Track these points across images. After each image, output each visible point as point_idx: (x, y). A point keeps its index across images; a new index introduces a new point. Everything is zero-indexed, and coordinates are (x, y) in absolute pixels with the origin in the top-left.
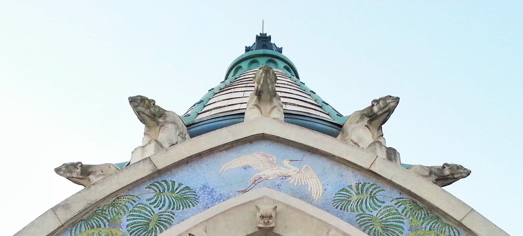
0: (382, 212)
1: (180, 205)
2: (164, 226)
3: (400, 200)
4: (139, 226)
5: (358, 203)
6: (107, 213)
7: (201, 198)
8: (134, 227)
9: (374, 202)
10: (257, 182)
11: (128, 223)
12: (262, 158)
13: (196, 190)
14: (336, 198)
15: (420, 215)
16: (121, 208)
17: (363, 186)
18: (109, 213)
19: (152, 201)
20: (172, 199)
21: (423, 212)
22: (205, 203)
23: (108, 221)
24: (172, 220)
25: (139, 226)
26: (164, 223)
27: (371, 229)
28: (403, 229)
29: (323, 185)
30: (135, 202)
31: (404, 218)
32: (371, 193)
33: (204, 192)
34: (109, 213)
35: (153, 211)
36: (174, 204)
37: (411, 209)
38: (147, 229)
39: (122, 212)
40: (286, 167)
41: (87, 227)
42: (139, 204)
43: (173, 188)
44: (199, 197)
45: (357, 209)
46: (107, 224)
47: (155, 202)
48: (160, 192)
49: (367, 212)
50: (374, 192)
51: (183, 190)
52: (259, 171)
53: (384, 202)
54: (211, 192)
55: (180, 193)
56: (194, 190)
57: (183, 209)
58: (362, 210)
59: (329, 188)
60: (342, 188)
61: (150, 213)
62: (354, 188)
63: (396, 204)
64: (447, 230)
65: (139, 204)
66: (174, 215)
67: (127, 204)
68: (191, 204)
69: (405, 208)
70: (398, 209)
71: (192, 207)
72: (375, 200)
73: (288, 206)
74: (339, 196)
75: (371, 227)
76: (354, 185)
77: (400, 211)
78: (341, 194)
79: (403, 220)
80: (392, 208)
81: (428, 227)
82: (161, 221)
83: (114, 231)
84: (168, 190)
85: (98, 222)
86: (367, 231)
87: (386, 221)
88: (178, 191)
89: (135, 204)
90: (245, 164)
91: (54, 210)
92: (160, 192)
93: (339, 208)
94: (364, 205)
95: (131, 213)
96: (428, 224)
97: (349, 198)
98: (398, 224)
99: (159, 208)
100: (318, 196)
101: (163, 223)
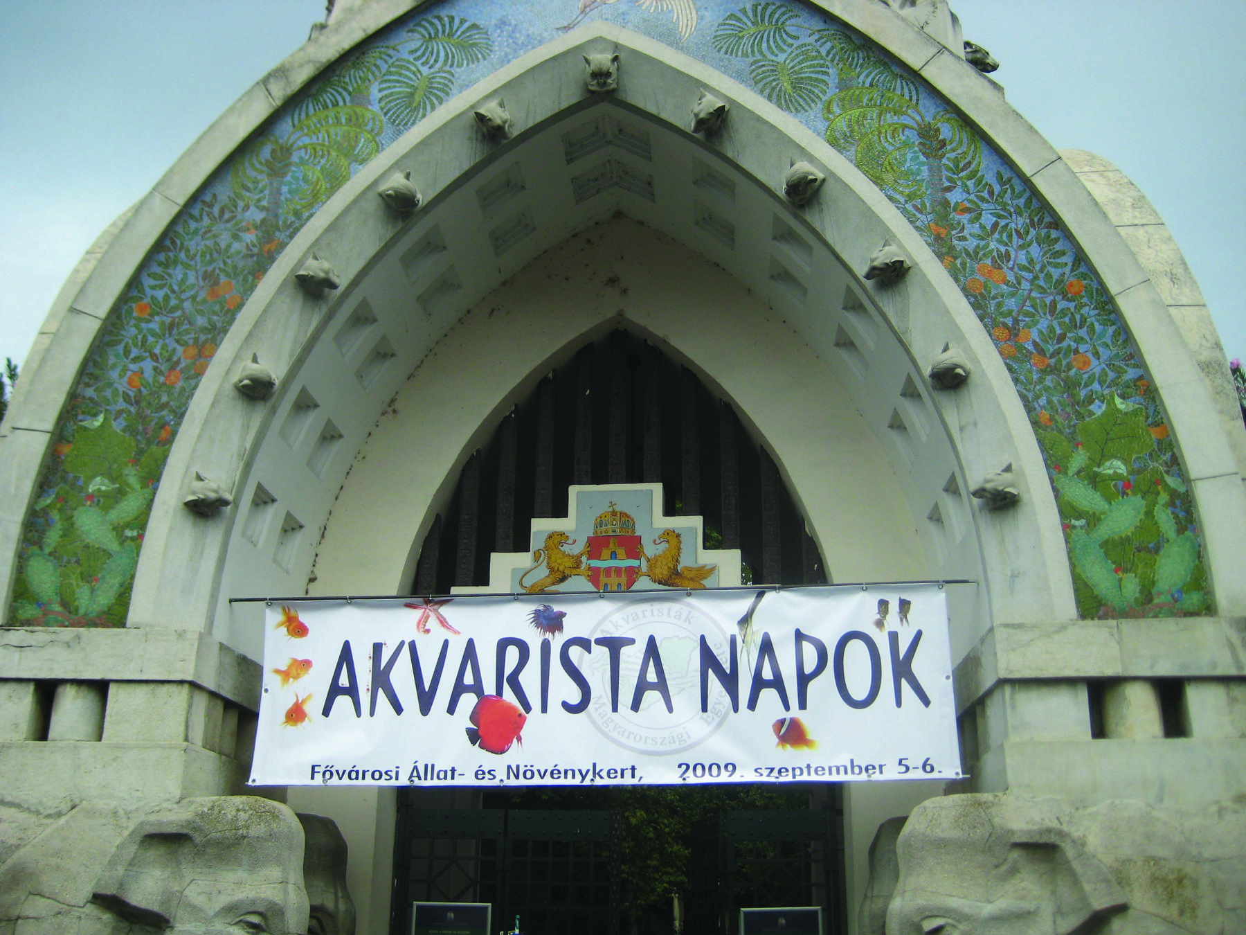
0: (793, 55)
1: (462, 59)
2: (437, 97)
3: (825, 33)
4: (398, 99)
5: (754, 40)
6: (347, 80)
7: (496, 44)
8: (390, 102)
9: (781, 37)
10: (588, 10)
11: (380, 95)
13: (488, 30)
14: (719, 33)
15: (856, 59)
16: (368, 69)
17: (765, 9)
18: (350, 80)
19: (419, 53)
20: (451, 49)
21: (861, 55)
22: (503, 53)
23: (350, 94)
24: (451, 86)
25: (398, 99)
26: (439, 93)
27: (774, 89)
30: (391, 57)
31: (830, 65)
32: (777, 21)
33: (502, 32)
34: (350, 80)
35: (419, 71)
36: (453, 57)
37: (842, 49)
38: (411, 104)
39: (371, 77)
41: (317, 108)
42: (397, 60)
43: (451, 27)
44: (493, 42)
45: (753, 52)
46: (348, 98)
47: (423, 54)
48: (430, 36)
50: (782, 20)
51: (469, 29)
54: (513, 32)
55: (462, 37)
56: (485, 31)
57: (468, 64)
58: (761, 52)
60: (729, 14)
61: (416, 76)
62: (750, 14)
63: (817, 41)
64: (898, 86)
65: (397, 60)
66: (453, 76)
67: (379, 62)
68: (480, 56)
69: (833, 48)
70: (820, 49)
71: (481, 60)
72: (784, 35)
74: (723, 30)
75: (774, 83)
76: (748, 7)
77: (824, 53)
78: (728, 24)
79: (827, 70)
80: (810, 48)
81: (868, 81)
82: (433, 88)
83: (359, 110)
84: (444, 32)
85: (334, 97)
86: (767, 91)
88: (459, 33)
89: (390, 61)
91: (265, 81)
92: (430, 34)
93: (723, 50)
94: (764, 45)
95: (386, 78)
96: (867, 76)
97: (740, 32)
98: (820, 76)
99: (429, 66)
100: (689, 30)
101: (436, 91)
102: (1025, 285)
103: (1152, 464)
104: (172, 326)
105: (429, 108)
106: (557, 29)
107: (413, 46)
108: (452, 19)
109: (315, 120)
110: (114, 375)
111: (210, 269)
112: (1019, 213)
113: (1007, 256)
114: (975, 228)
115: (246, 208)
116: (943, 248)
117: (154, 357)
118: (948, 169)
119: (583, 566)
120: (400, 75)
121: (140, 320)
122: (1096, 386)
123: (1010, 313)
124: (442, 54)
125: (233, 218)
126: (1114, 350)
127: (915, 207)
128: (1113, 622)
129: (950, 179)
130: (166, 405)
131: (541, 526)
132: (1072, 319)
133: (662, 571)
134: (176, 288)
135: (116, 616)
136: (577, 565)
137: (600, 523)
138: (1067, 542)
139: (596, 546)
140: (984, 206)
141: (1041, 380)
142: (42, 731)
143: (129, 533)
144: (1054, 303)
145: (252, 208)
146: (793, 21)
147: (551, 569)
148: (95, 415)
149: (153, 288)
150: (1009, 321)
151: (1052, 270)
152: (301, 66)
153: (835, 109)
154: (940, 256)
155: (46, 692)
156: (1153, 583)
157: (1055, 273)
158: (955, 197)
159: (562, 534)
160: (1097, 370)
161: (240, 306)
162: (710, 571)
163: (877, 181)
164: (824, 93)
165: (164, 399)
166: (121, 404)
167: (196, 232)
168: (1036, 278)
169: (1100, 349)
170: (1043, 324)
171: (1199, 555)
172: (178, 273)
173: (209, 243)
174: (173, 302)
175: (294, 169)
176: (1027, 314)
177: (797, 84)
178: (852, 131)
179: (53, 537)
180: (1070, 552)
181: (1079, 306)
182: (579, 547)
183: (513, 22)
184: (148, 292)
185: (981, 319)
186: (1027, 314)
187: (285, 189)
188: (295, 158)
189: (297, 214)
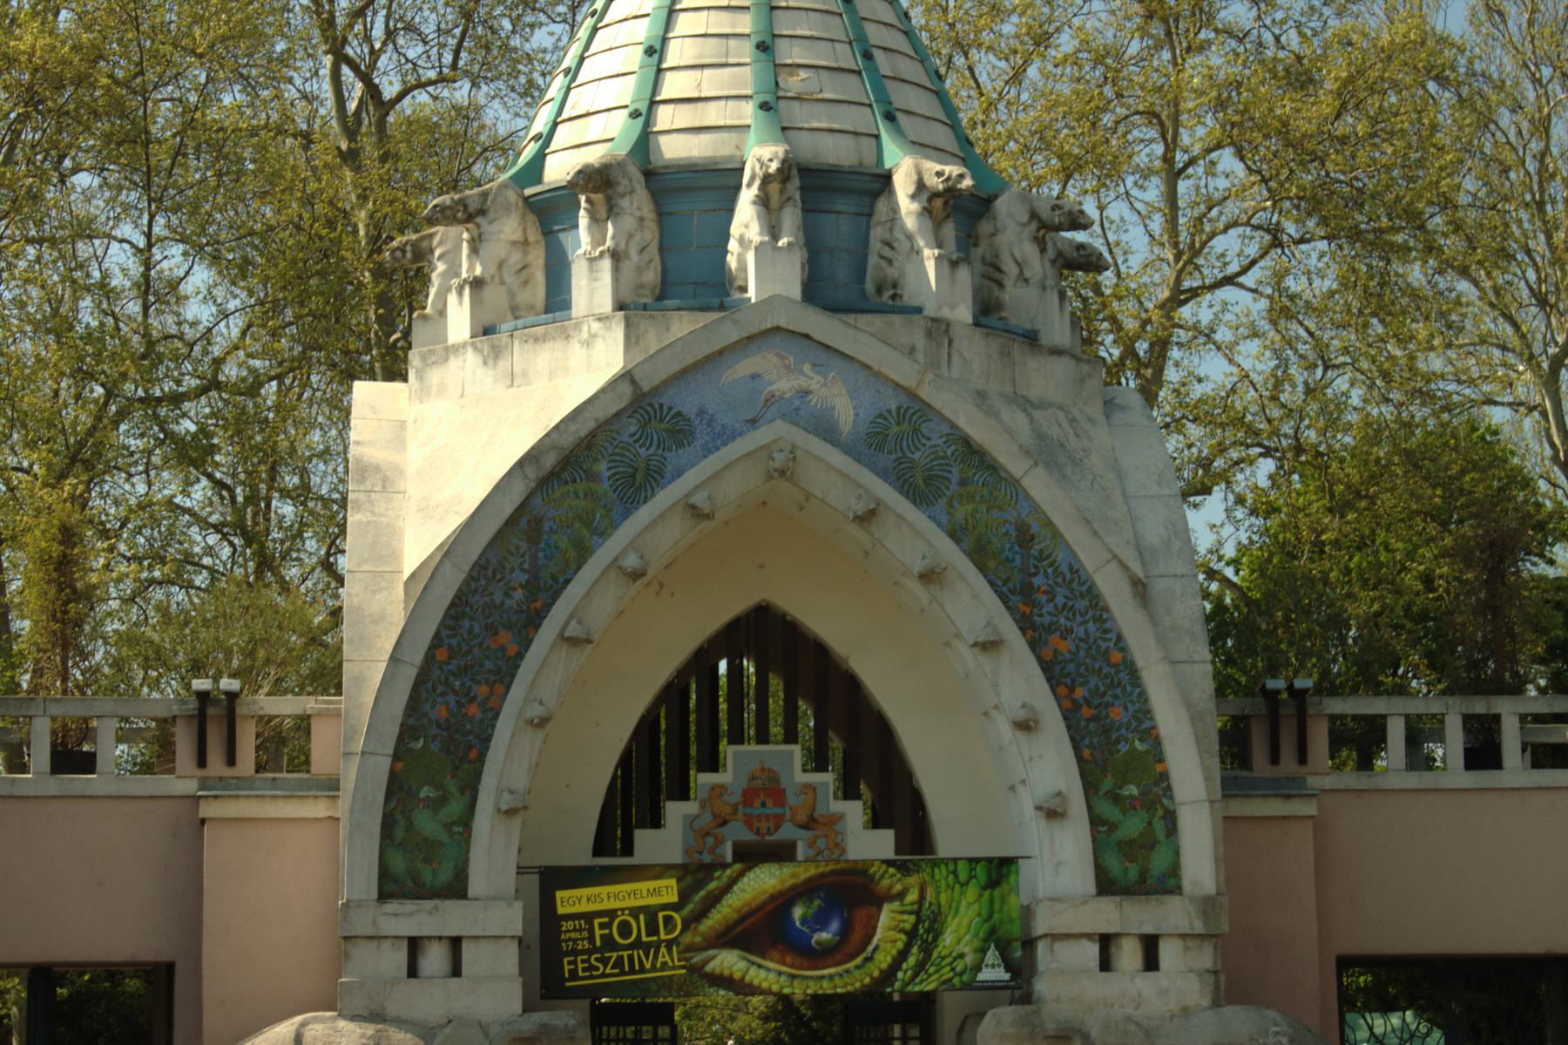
2: (655, 480)
11: (608, 474)
12: (775, 360)
28: (950, 482)
29: (855, 408)
40: (807, 376)
47: (640, 438)
49: (908, 454)
51: (673, 417)
52: (771, 383)
53: (929, 439)
59: (861, 411)
62: (894, 414)
73: (807, 452)
76: (893, 407)
77: (949, 454)
86: (906, 487)
87: (931, 469)
90: (752, 370)
94: (905, 443)
102: (1082, 653)
103: (1155, 789)
104: (466, 667)
105: (649, 493)
106: (747, 421)
107: (633, 429)
108: (661, 406)
109: (558, 493)
110: (427, 707)
111: (490, 620)
112: (1083, 597)
113: (1071, 631)
114: (1050, 608)
115: (512, 570)
116: (1025, 624)
117: (454, 691)
118: (1035, 558)
119: (740, 813)
120: (623, 456)
121: (440, 662)
122: (1123, 731)
123: (1069, 675)
124: (655, 437)
125: (503, 578)
126: (1138, 706)
127: (1009, 590)
128: (1118, 898)
129: (1036, 567)
130: (470, 732)
131: (702, 780)
132: (1112, 680)
133: (802, 817)
134: (465, 636)
135: (457, 889)
136: (735, 812)
137: (753, 778)
138: (1093, 842)
139: (749, 796)
140: (1058, 589)
141: (1086, 726)
142: (413, 972)
143: (456, 829)
144: (1100, 669)
145: (517, 571)
146: (927, 424)
147: (715, 816)
148: (417, 739)
149: (448, 637)
150: (1069, 681)
151: (1101, 643)
152: (548, 451)
153: (956, 503)
154: (1023, 630)
155: (415, 945)
156: (1148, 870)
157: (1104, 645)
158: (1038, 581)
159: (722, 787)
160: (1125, 720)
161: (520, 656)
162: (840, 818)
163: (982, 568)
164: (948, 488)
165: (468, 727)
166: (435, 731)
167: (476, 591)
168: (1090, 648)
169: (1129, 705)
170: (1094, 681)
172: (466, 623)
173: (487, 599)
174: (465, 648)
175: (545, 536)
176: (1081, 676)
177: (928, 480)
178: (967, 523)
179: (399, 832)
180: (1095, 849)
181: (1118, 672)
182: (736, 797)
183: (711, 412)
184: (447, 641)
185: (1048, 680)
186: (1081, 676)
187: (541, 555)
188: (546, 527)
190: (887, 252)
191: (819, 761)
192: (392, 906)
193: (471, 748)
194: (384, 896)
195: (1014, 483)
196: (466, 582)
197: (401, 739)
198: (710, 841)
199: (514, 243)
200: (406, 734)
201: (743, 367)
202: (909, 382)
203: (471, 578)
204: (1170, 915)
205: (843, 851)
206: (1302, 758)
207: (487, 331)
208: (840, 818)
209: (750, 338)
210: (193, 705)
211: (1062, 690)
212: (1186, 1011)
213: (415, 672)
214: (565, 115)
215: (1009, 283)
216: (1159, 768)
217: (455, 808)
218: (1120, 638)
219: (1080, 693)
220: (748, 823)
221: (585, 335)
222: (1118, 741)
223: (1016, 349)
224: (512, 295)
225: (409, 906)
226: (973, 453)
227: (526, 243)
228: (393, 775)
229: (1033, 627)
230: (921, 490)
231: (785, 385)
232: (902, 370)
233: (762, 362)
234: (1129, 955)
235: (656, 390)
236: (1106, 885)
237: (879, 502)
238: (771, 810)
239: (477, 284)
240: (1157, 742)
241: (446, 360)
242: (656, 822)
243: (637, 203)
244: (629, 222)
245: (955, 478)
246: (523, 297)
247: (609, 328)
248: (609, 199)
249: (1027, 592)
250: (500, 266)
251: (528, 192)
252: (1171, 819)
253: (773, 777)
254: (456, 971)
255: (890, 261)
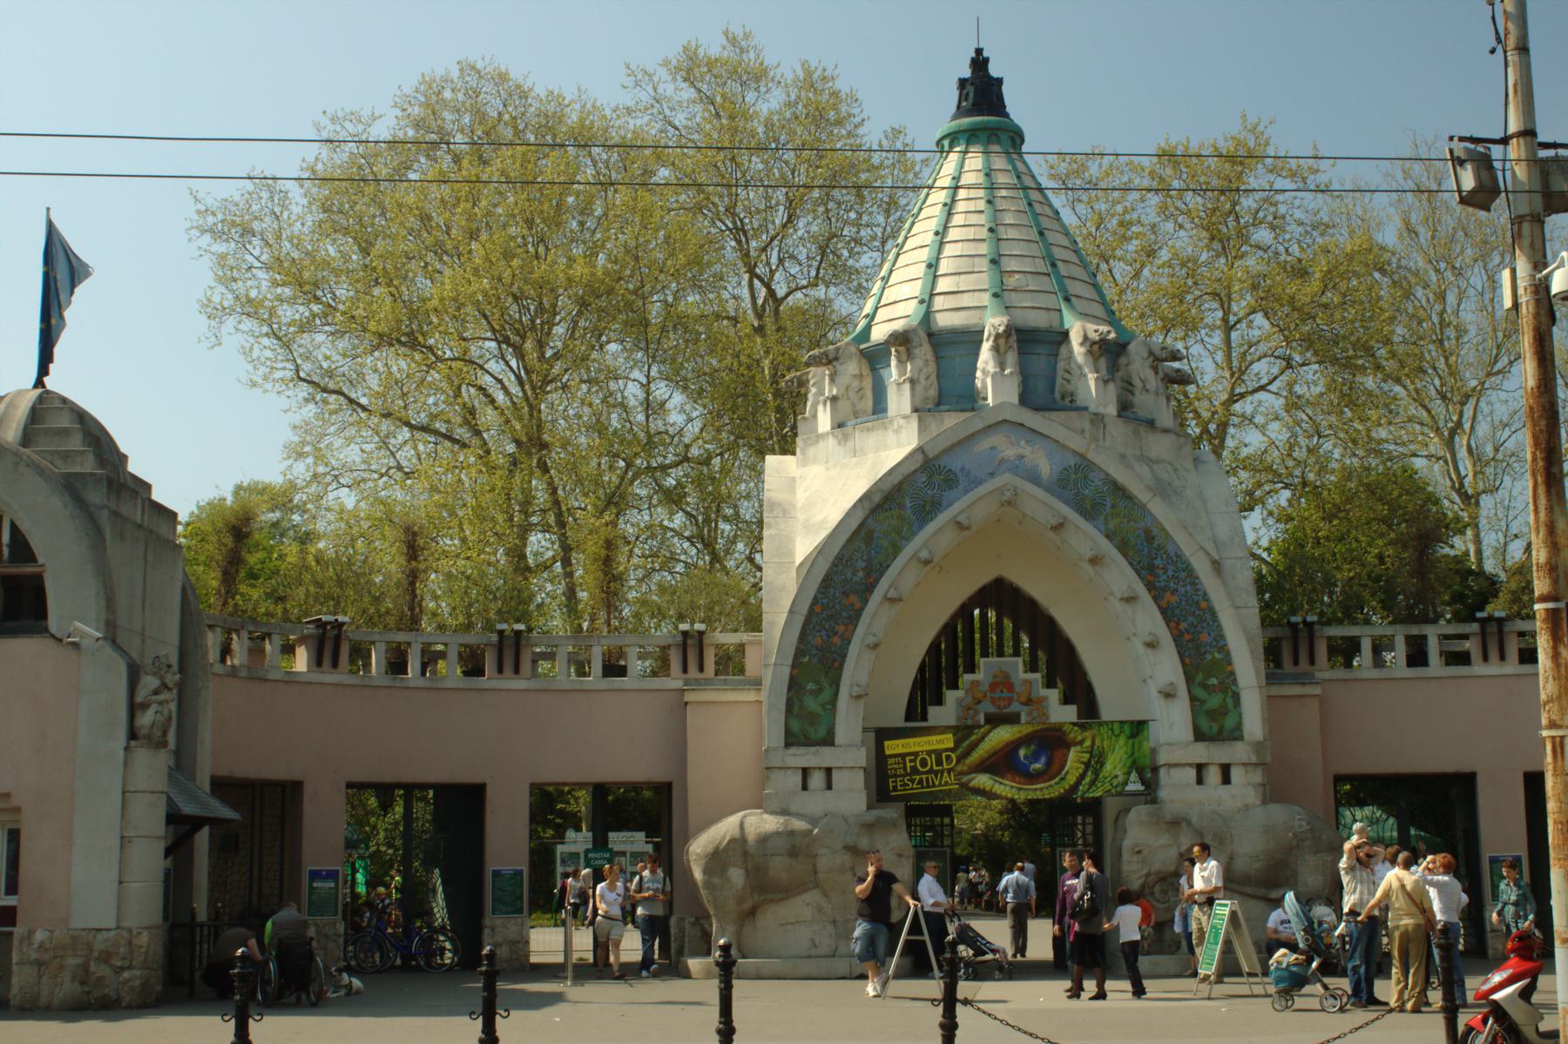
110: (810, 638)
113: (1176, 590)
116: (1150, 587)
131: (967, 678)
133: (1023, 699)
135: (828, 741)
137: (995, 677)
139: (993, 687)
142: (805, 787)
154: (1149, 590)
155: (805, 772)
158: (1158, 562)
161: (862, 609)
162: (1045, 699)
163: (1125, 555)
166: (815, 652)
170: (1191, 619)
171: (1240, 717)
172: (831, 591)
177: (1094, 505)
179: (796, 708)
182: (985, 687)
185: (1165, 618)
188: (876, 535)
189: (881, 565)
190: (1067, 376)
191: (1032, 667)
192: (793, 750)
193: (834, 661)
194: (788, 745)
195: (1143, 507)
196: (831, 568)
197: (796, 656)
198: (971, 712)
199: (855, 376)
200: (799, 653)
201: (985, 444)
202: (1081, 450)
203: (834, 565)
204: (1237, 753)
205: (1048, 718)
206: (1312, 662)
207: (840, 426)
208: (1045, 699)
209: (989, 426)
210: (679, 638)
211: (1173, 624)
212: (1247, 807)
213: (803, 618)
214: (882, 303)
215: (1137, 392)
216: (1229, 668)
217: (827, 694)
218: (1205, 594)
219: (1183, 626)
220: (993, 701)
221: (896, 426)
222: (1205, 653)
223: (1142, 430)
224: (854, 405)
225: (802, 750)
226: (1118, 490)
227: (861, 375)
228: (792, 678)
229: (1155, 588)
230: (1089, 511)
231: (1010, 453)
232: (1076, 443)
233: (997, 440)
234: (1213, 775)
235: (937, 457)
236: (1199, 736)
237: (1065, 519)
238: (1006, 694)
239: (834, 399)
240: (1228, 654)
241: (817, 442)
242: (939, 701)
243: (924, 351)
244: (919, 362)
245: (1108, 504)
246: (860, 406)
247: (909, 423)
248: (908, 350)
249: (1151, 568)
250: (847, 389)
251: (862, 347)
252: (1236, 698)
253: (1006, 676)
254: (829, 787)
255: (1069, 381)
